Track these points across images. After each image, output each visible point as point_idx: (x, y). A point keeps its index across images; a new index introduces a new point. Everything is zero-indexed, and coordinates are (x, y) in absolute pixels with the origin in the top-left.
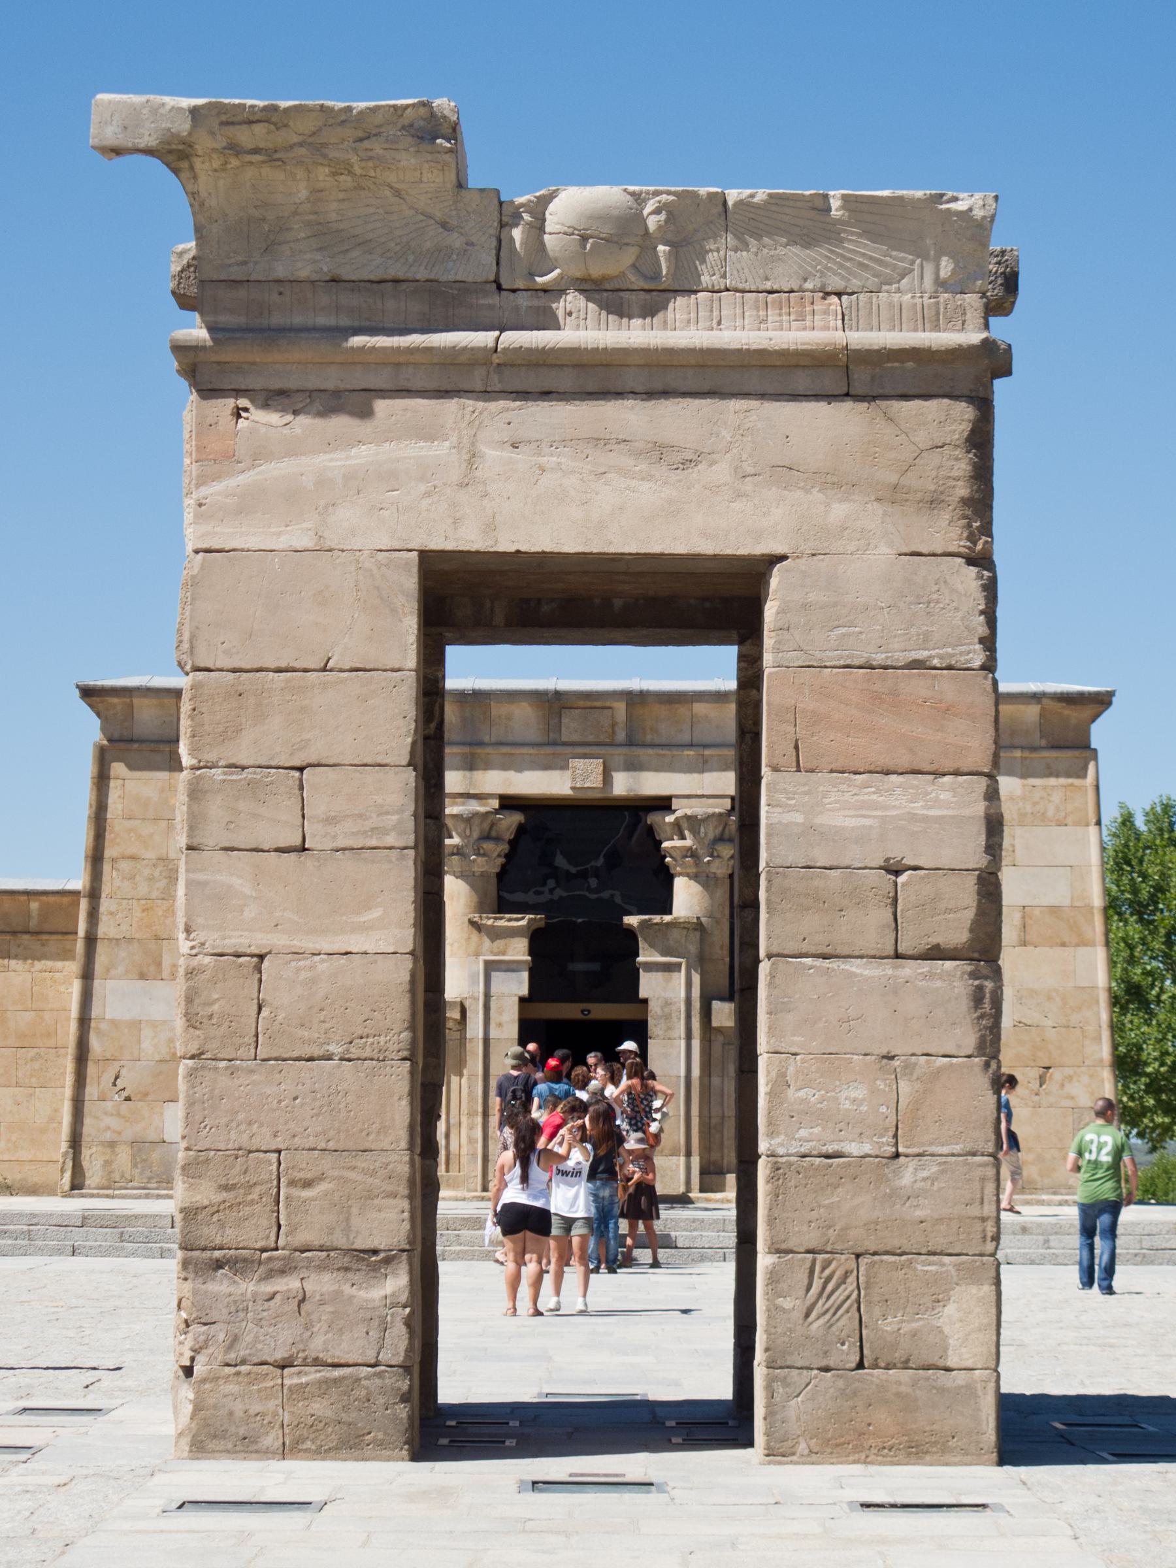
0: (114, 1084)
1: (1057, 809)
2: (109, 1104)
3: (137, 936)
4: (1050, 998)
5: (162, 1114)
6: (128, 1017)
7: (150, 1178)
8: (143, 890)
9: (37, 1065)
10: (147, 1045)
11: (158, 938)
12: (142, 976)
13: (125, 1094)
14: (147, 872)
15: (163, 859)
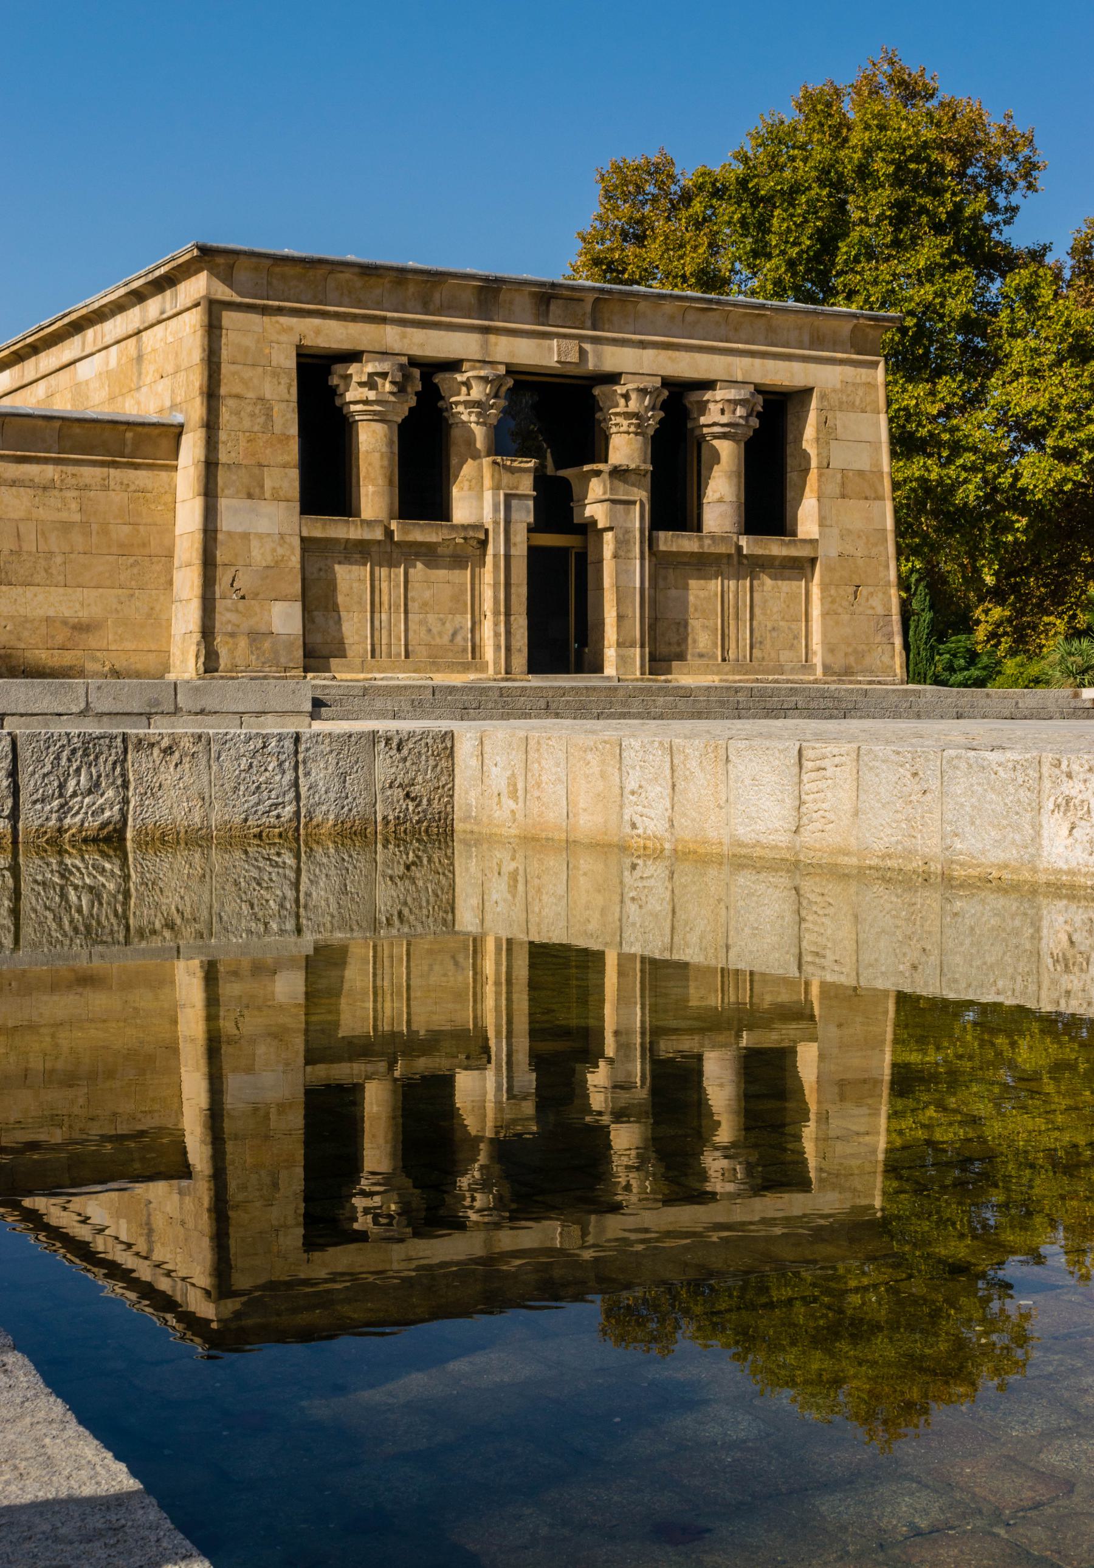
0: (232, 585)
1: (861, 401)
2: (229, 601)
3: (244, 462)
4: (859, 537)
5: (270, 611)
6: (240, 530)
7: (264, 663)
8: (247, 424)
9: (135, 571)
10: (256, 553)
11: (260, 465)
12: (250, 496)
13: (241, 593)
14: (249, 409)
15: (261, 399)
